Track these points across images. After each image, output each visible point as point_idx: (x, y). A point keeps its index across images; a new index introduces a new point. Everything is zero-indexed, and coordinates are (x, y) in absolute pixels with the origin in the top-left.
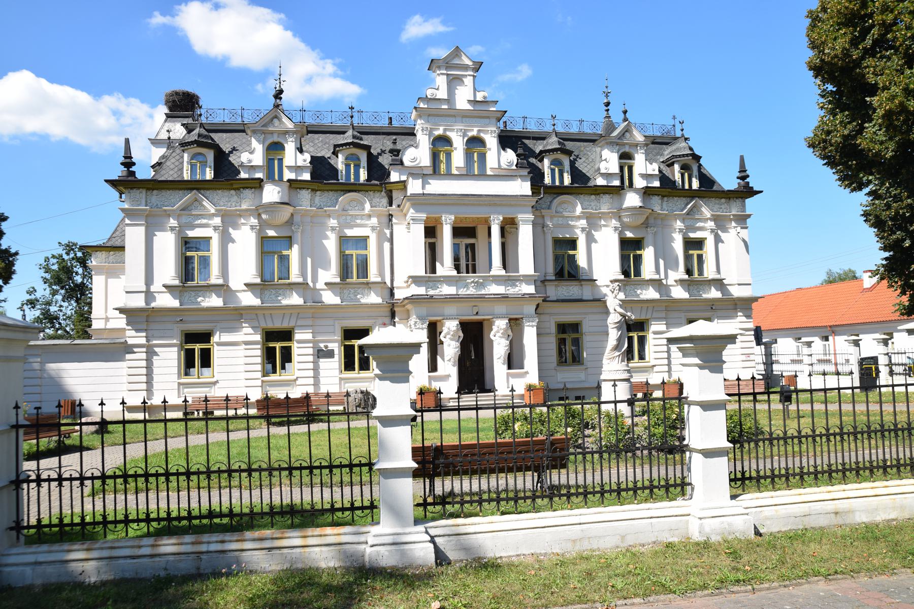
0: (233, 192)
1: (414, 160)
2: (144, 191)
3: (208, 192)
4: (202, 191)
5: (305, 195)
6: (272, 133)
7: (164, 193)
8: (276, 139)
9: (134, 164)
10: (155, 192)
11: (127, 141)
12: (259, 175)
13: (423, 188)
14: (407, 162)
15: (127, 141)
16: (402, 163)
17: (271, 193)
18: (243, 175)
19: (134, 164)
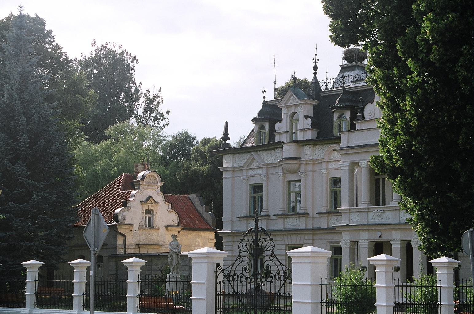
0: (273, 151)
1: (371, 113)
2: (232, 156)
3: (261, 152)
4: (259, 153)
5: (308, 149)
6: (291, 106)
7: (241, 155)
8: (292, 110)
9: (229, 139)
10: (237, 155)
11: (227, 123)
12: (284, 138)
13: (348, 142)
14: (367, 117)
15: (227, 123)
16: (363, 117)
17: (289, 151)
18: (277, 139)
19: (229, 139)
